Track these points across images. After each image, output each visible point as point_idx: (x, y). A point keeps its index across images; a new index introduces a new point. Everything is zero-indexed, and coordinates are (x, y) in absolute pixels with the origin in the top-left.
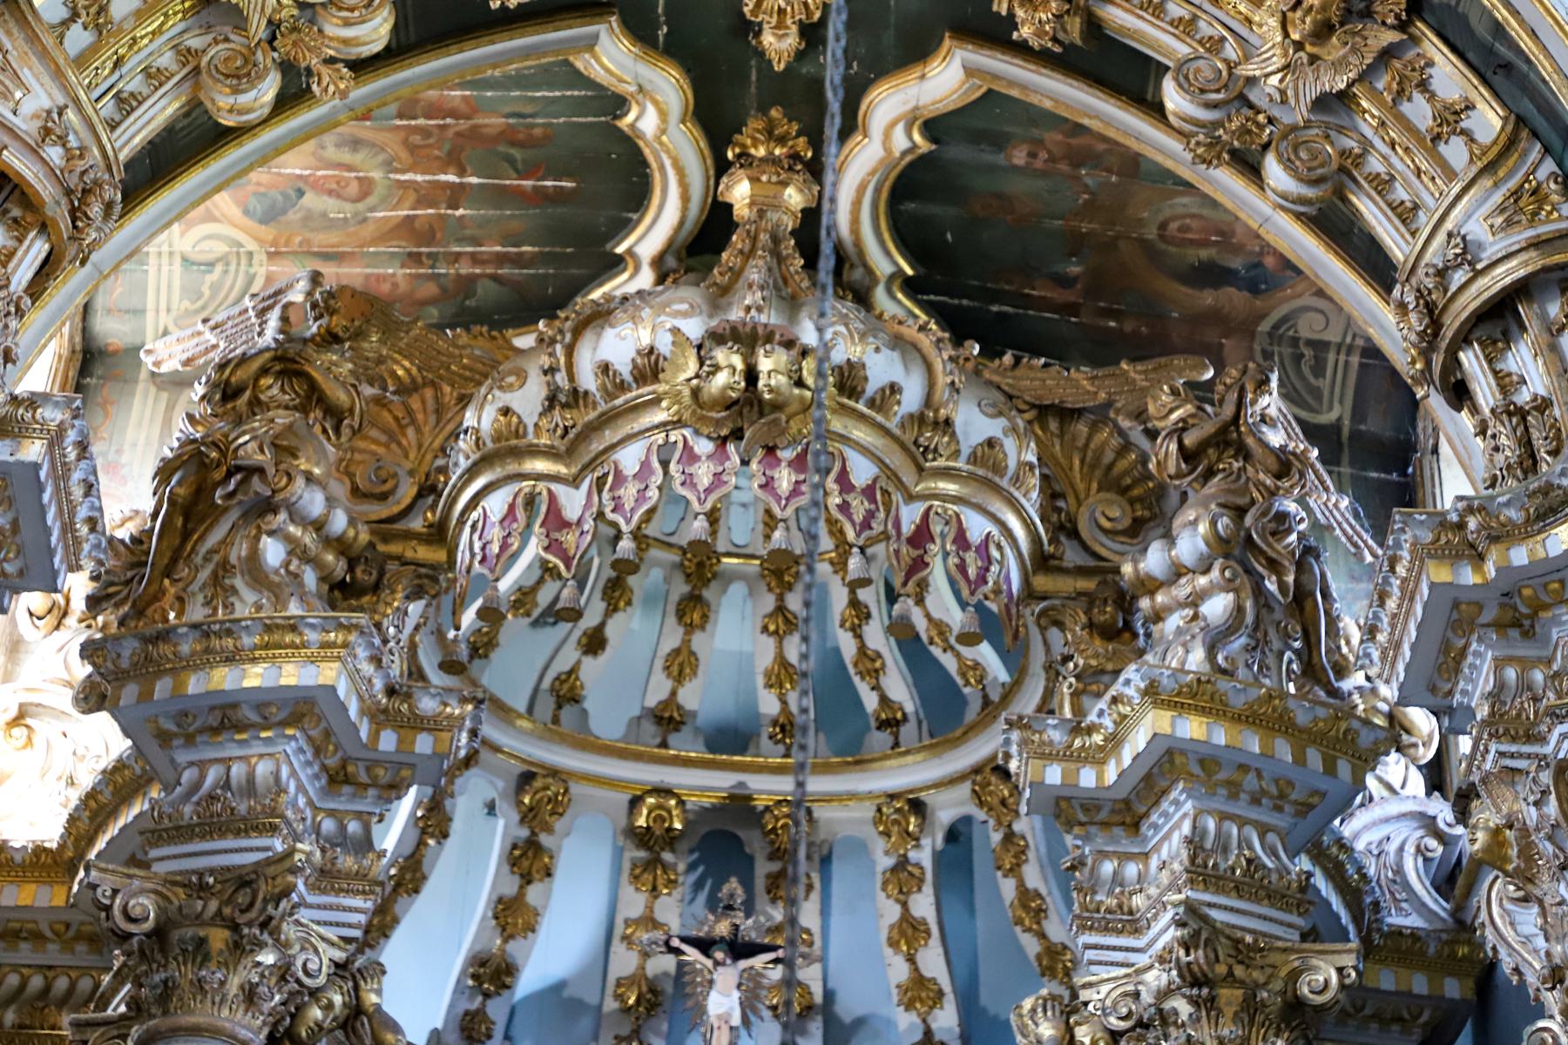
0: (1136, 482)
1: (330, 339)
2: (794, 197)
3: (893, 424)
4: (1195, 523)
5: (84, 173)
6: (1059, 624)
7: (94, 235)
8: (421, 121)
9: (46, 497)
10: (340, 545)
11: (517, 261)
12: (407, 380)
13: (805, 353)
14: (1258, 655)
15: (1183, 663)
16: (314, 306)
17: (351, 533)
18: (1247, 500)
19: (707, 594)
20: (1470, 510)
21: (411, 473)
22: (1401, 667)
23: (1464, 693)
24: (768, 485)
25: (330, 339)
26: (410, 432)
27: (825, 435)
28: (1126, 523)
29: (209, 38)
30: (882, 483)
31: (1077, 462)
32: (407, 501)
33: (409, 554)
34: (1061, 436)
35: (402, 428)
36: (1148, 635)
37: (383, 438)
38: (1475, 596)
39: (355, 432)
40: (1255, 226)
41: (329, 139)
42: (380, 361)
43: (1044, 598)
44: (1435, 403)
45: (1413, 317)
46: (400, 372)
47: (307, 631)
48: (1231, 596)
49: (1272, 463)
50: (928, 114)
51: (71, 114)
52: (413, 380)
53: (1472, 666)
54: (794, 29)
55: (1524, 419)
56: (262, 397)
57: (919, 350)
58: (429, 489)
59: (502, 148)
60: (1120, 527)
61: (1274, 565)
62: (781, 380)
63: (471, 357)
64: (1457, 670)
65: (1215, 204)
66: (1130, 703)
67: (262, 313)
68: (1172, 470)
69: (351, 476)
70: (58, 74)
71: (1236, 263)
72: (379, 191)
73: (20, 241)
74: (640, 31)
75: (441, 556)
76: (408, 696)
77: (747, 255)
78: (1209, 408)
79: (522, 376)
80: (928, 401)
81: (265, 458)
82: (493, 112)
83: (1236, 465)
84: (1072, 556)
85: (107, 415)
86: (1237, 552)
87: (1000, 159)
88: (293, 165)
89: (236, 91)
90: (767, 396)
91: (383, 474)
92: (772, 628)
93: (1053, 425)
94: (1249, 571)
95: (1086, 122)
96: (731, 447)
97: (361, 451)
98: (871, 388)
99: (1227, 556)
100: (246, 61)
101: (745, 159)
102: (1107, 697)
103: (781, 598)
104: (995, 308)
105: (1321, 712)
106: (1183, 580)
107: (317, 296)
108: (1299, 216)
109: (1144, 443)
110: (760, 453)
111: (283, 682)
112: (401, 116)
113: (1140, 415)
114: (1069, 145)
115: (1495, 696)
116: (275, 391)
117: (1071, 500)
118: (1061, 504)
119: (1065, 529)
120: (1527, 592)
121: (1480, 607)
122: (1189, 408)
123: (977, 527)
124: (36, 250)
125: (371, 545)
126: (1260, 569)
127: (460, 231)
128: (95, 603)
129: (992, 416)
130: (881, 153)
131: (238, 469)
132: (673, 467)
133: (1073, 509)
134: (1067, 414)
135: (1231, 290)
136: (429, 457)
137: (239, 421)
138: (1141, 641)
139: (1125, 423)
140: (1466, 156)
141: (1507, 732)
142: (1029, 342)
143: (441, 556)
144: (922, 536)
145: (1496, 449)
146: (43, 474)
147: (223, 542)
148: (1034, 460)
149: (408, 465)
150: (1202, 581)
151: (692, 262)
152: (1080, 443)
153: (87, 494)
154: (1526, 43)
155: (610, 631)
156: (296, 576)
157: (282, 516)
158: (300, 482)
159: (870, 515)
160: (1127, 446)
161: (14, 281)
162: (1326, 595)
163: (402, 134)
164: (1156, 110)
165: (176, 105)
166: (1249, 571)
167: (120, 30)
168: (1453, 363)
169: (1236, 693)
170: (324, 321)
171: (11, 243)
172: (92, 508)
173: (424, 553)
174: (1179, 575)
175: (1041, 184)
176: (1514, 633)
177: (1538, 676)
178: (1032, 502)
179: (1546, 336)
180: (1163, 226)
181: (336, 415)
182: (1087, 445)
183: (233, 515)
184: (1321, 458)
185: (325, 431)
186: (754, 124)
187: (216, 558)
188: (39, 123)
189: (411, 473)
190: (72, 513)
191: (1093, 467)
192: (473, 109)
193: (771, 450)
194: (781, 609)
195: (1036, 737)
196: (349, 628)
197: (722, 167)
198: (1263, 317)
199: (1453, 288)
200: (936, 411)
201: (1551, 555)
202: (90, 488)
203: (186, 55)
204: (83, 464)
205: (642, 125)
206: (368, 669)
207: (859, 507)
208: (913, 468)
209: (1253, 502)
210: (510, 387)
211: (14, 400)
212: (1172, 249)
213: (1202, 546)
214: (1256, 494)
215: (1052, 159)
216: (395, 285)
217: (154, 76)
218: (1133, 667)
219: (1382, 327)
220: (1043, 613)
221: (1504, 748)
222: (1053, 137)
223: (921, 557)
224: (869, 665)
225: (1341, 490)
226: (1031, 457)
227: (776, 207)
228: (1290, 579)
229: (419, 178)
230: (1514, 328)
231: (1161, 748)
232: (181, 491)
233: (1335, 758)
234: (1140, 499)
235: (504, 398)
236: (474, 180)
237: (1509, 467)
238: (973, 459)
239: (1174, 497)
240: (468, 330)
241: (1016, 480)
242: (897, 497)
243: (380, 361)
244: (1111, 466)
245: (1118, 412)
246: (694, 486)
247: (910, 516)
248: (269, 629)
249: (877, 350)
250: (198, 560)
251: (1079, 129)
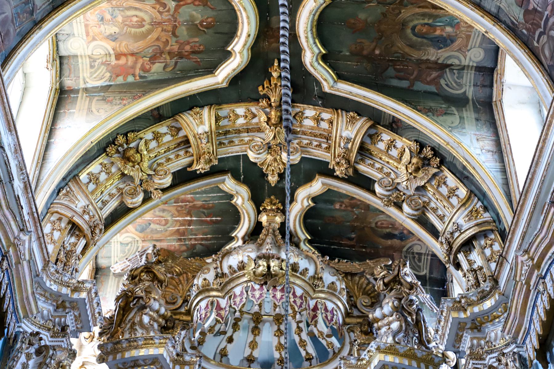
0: (372, 292)
1: (159, 262)
2: (278, 219)
3: (307, 279)
4: (388, 303)
5: (94, 222)
6: (353, 331)
7: (97, 238)
8: (180, 204)
9: (87, 307)
10: (163, 317)
11: (206, 239)
12: (179, 272)
13: (283, 261)
14: (406, 338)
15: (386, 341)
16: (154, 254)
17: (166, 313)
18: (402, 296)
19: (259, 326)
20: (462, 297)
21: (181, 297)
22: (445, 341)
23: (463, 347)
24: (274, 296)
25: (159, 262)
26: (180, 286)
27: (289, 283)
28: (370, 303)
29: (125, 185)
30: (304, 295)
31: (356, 287)
32: (180, 304)
33: (181, 318)
34: (352, 280)
35: (178, 285)
36: (377, 334)
37: (173, 288)
38: (464, 321)
39: (166, 286)
40: (401, 222)
41: (157, 210)
42: (172, 267)
43: (348, 324)
44: (451, 268)
45: (445, 246)
46: (177, 270)
47: (155, 340)
48: (399, 322)
49: (408, 286)
50: (313, 196)
51: (90, 207)
52: (181, 272)
53: (465, 340)
54: (277, 175)
55: (476, 272)
56: (142, 278)
57: (313, 259)
58: (186, 301)
59: (201, 210)
60: (368, 305)
61: (410, 314)
62: (277, 268)
63: (195, 265)
64: (461, 341)
65: (390, 217)
66: (373, 352)
67: (141, 256)
68: (381, 289)
69: (165, 298)
70: (87, 196)
71: (396, 233)
72: (170, 223)
73: (79, 240)
74: (236, 177)
75: (189, 318)
76: (182, 356)
77: (266, 235)
78: (391, 272)
79: (209, 270)
80: (316, 273)
81: (143, 294)
82: (199, 201)
83: (399, 287)
84: (356, 313)
85: (102, 285)
86: (400, 310)
87: (332, 207)
88: (148, 217)
89: (132, 198)
90: (273, 273)
91: (174, 297)
92: (277, 334)
93: (349, 278)
94: (403, 316)
95: (355, 196)
96: (264, 287)
97: (168, 291)
98: (301, 270)
99: (397, 312)
100: (135, 190)
101: (265, 210)
102: (367, 351)
103: (279, 326)
104: (332, 247)
105: (424, 353)
106: (386, 319)
107: (155, 251)
108: (413, 219)
109: (374, 282)
110: (272, 288)
111: (150, 353)
112: (175, 203)
113: (372, 274)
114: (351, 203)
115: (471, 348)
116: (145, 276)
117: (355, 298)
118: (352, 299)
119: (353, 305)
120: (478, 319)
121: (466, 324)
122: (385, 272)
123: (330, 306)
124: (83, 242)
125: (171, 316)
126: (406, 315)
127: (192, 232)
128: (101, 334)
129: (333, 276)
130: (301, 207)
131: (136, 297)
132: (249, 292)
133: (355, 300)
134: (353, 275)
135: (395, 240)
136: (185, 292)
137: (136, 285)
138: (375, 335)
139: (368, 277)
140: (457, 202)
141: (475, 358)
142: (342, 256)
143: (189, 318)
144: (315, 309)
145: (469, 281)
146: (86, 301)
147: (133, 317)
148: (345, 287)
149: (180, 295)
150: (391, 319)
151: (252, 238)
152: (357, 282)
153: (98, 306)
154: (472, 171)
155: (234, 337)
156: (152, 325)
157: (148, 309)
158: (152, 300)
159: (302, 303)
160: (369, 283)
161: (77, 251)
162: (424, 321)
163: (175, 208)
164: (373, 192)
165: (117, 203)
166: (403, 316)
167: (102, 184)
168: (456, 258)
169: (401, 349)
170: (157, 258)
171: (76, 241)
172: (99, 309)
173: (185, 318)
174: (384, 317)
175: (344, 213)
176: (476, 331)
177: (483, 342)
178: (344, 298)
179: (481, 250)
180: (376, 223)
181: (161, 282)
182: (358, 283)
183: (136, 310)
184: (421, 284)
185: (158, 287)
186: (267, 200)
187: (131, 321)
188: (82, 209)
189: (181, 297)
190: (94, 311)
191: (360, 288)
192: (194, 200)
193: (275, 287)
194: (279, 329)
195: (348, 362)
196: (166, 339)
197: (259, 212)
198: (404, 247)
199: (455, 237)
200: (318, 275)
201: (485, 309)
202: (98, 304)
203: (119, 190)
204: (96, 298)
205: (238, 202)
206: (171, 349)
207: (299, 301)
208: (312, 291)
209: (404, 297)
210: (206, 273)
211: (78, 282)
212: (380, 230)
213: (390, 309)
214: (404, 295)
215: (346, 206)
216: (175, 247)
217: (111, 196)
218: (373, 342)
219: (436, 249)
220: (348, 328)
221: (474, 362)
222: (346, 201)
223: (315, 314)
224: (303, 344)
225: (427, 293)
226: (344, 286)
227: (274, 222)
228: (414, 317)
229: (180, 219)
230: (472, 248)
231: (381, 364)
232: (122, 304)
233: (428, 366)
234: (373, 297)
235: (204, 276)
236: (195, 219)
237: (472, 285)
238: (328, 287)
239: (382, 296)
240: (194, 258)
241: (340, 293)
242: (308, 298)
243: (172, 267)
244: (365, 288)
245: (366, 274)
246: (255, 297)
247: (312, 303)
248: (145, 339)
249: (302, 259)
250: (127, 322)
251: (353, 198)
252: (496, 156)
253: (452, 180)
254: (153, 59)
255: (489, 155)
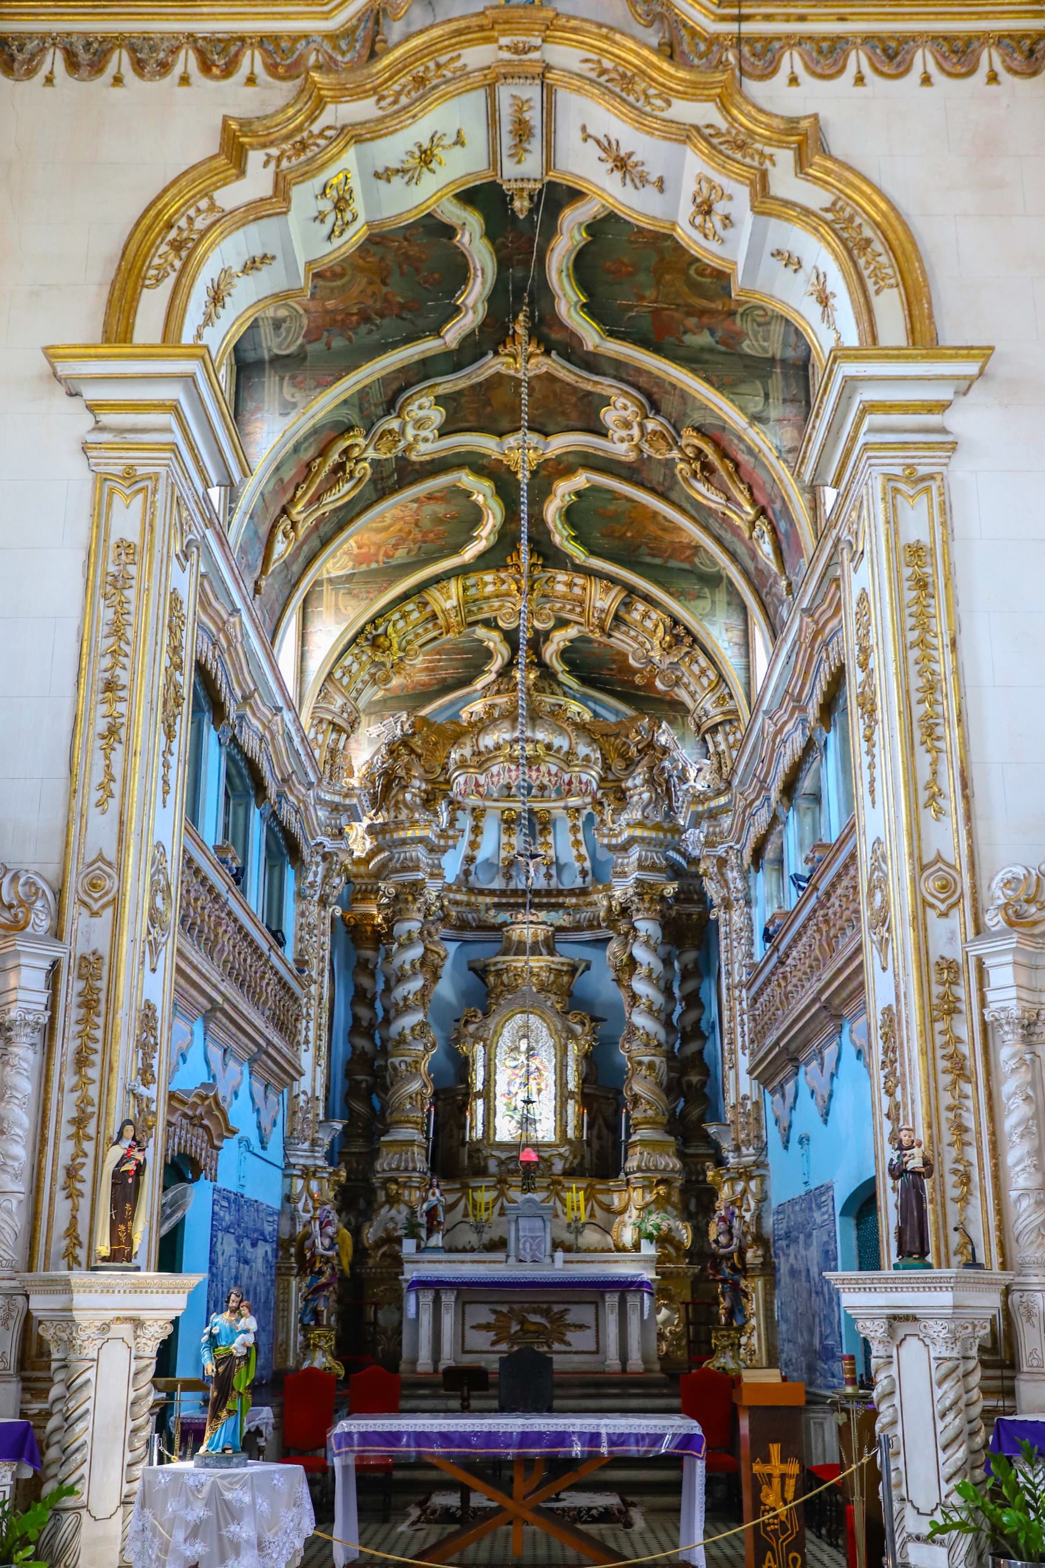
61: (660, 785)
123: (585, 777)
247: (567, 777)
252: (743, 651)
253: (703, 661)
254: (395, 547)
255: (736, 649)
